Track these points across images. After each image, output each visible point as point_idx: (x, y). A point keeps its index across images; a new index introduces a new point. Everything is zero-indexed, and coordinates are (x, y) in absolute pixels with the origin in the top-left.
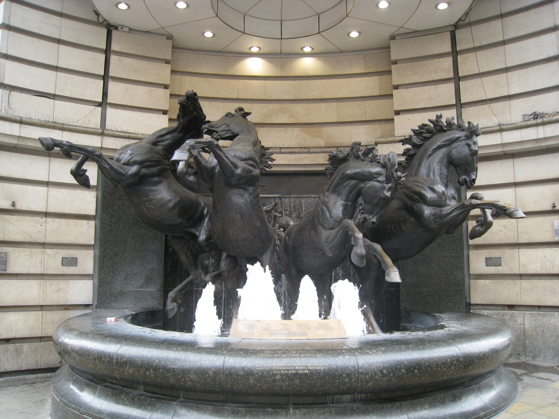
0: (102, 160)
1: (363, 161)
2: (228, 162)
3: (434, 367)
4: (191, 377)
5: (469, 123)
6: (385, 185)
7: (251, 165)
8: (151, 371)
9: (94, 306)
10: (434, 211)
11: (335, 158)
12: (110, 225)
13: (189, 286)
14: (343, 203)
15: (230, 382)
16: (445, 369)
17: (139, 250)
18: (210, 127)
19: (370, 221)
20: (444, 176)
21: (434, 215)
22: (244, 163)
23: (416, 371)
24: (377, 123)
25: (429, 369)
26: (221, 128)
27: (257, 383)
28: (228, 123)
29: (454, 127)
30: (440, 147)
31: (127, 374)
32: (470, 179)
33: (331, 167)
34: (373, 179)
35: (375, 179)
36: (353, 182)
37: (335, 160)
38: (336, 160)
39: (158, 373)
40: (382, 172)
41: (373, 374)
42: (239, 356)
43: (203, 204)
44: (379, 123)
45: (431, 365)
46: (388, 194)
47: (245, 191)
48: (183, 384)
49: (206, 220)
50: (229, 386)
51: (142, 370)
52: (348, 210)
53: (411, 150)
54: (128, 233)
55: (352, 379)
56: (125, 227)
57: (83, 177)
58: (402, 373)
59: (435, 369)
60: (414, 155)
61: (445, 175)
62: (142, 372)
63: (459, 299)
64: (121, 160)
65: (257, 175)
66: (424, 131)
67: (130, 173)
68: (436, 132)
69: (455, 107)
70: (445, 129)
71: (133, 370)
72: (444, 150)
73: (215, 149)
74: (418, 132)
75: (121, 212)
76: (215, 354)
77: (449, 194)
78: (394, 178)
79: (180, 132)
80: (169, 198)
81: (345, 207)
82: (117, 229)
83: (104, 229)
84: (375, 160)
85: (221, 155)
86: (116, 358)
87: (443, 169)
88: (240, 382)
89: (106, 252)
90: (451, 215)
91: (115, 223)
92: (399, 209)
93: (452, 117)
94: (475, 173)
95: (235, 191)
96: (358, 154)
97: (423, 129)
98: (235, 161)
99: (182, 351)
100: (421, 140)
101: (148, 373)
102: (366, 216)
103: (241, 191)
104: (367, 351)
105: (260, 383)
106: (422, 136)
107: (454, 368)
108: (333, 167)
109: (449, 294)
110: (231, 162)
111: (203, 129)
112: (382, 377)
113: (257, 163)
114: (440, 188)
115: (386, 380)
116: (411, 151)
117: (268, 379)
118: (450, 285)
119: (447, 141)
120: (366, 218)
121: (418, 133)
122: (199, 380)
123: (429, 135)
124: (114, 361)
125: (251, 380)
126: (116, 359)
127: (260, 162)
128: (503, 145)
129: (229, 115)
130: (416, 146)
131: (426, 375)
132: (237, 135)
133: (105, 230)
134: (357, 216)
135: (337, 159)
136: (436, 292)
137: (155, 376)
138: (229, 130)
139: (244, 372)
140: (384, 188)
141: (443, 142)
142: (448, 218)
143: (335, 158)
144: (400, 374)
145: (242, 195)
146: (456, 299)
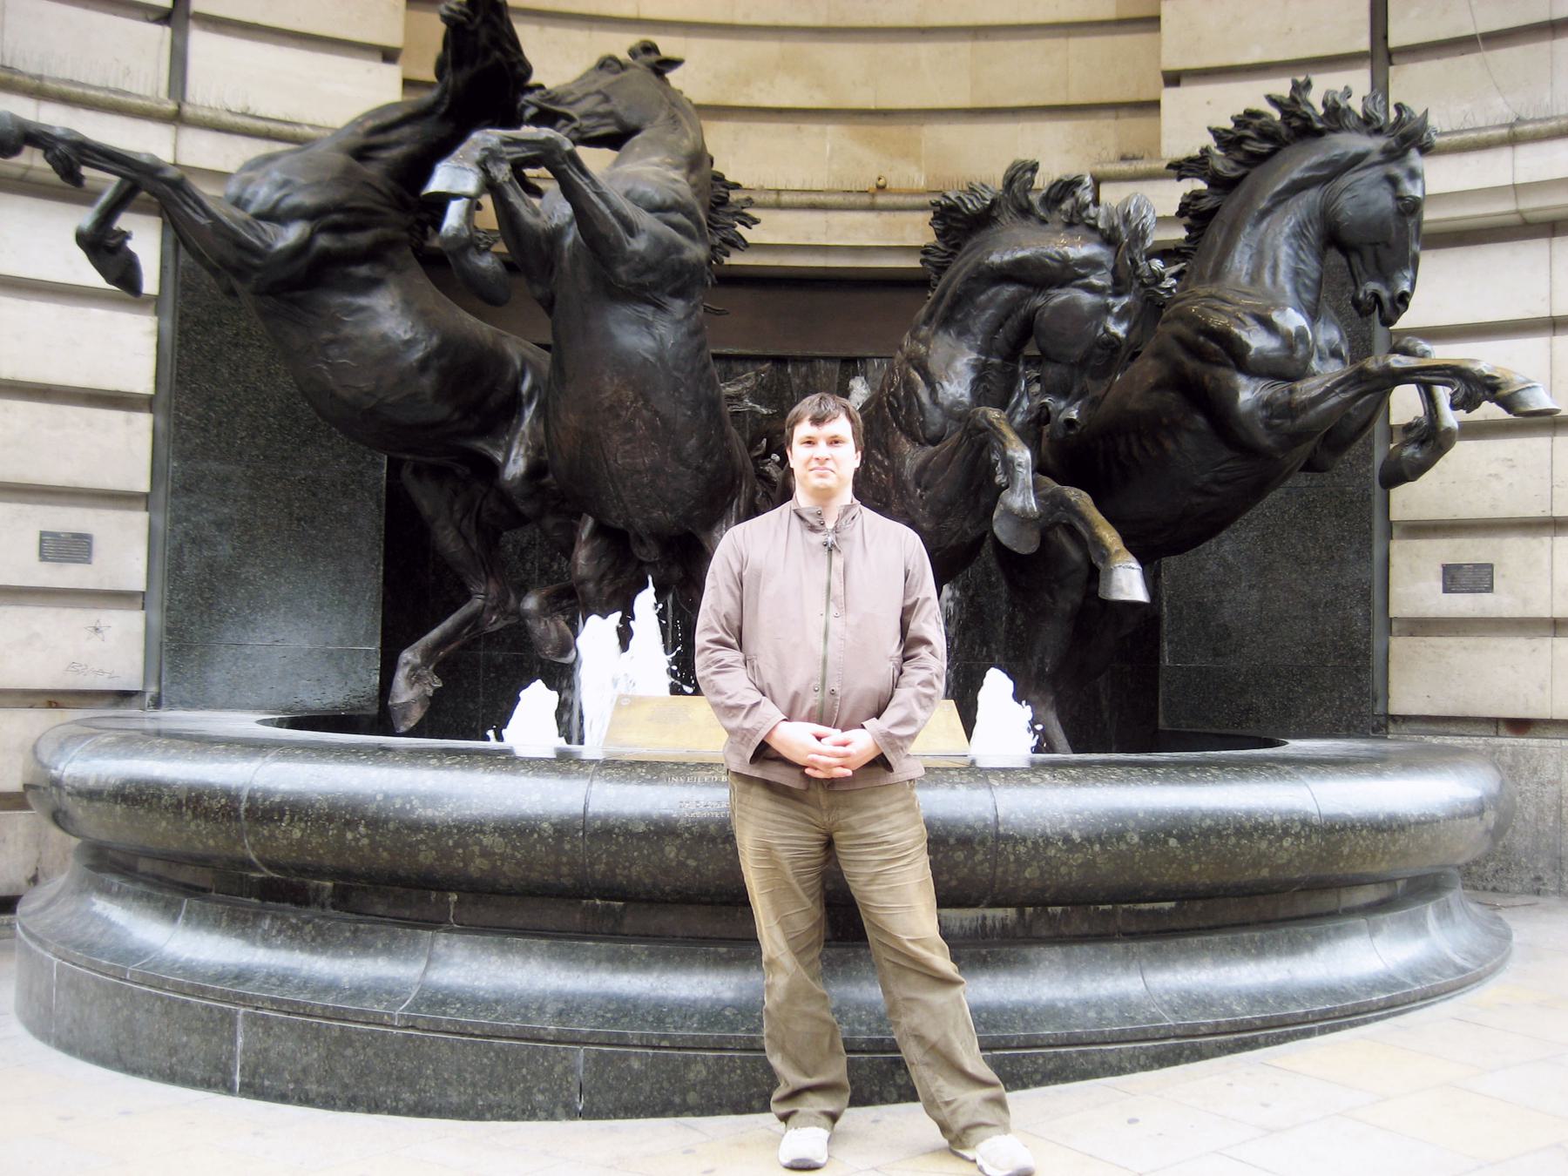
0: (188, 200)
1: (1043, 221)
2: (607, 212)
3: (1228, 835)
4: (486, 841)
5: (1400, 108)
6: (1111, 300)
7: (676, 227)
8: (362, 829)
9: (148, 697)
10: (1267, 394)
11: (954, 215)
12: (205, 430)
13: (466, 631)
14: (976, 360)
15: (604, 856)
16: (1264, 845)
17: (301, 514)
18: (546, 101)
19: (1061, 416)
20: (1307, 281)
21: (1267, 404)
22: (659, 218)
23: (1173, 842)
24: (1103, 114)
25: (1213, 840)
26: (587, 105)
27: (687, 858)
28: (604, 90)
29: (1350, 121)
30: (1297, 188)
31: (285, 842)
33: (941, 246)
34: (1072, 280)
35: (1079, 282)
36: (1008, 291)
37: (954, 219)
38: (959, 221)
39: (382, 835)
40: (1104, 259)
41: (1040, 840)
42: (632, 779)
43: (518, 363)
44: (1112, 113)
45: (1220, 828)
46: (1119, 330)
47: (659, 312)
48: (461, 865)
49: (529, 413)
50: (602, 867)
51: (332, 826)
52: (990, 381)
53: (1204, 197)
54: (265, 457)
55: (974, 855)
56: (253, 437)
58: (1128, 844)
59: (1233, 840)
60: (1213, 212)
61: (1309, 278)
62: (330, 833)
63: (1352, 700)
64: (248, 202)
65: (699, 261)
66: (1249, 133)
67: (280, 245)
68: (1288, 136)
69: (1368, 64)
70: (1319, 126)
71: (303, 830)
72: (1313, 195)
74: (1231, 136)
75: (240, 389)
76: (560, 773)
77: (1321, 343)
78: (1139, 277)
79: (445, 117)
80: (407, 336)
81: (981, 374)
82: (228, 444)
84: (1082, 220)
85: (585, 187)
86: (249, 798)
87: (1303, 256)
88: (636, 854)
90: (1323, 406)
91: (220, 423)
92: (1158, 387)
93: (1346, 88)
94: (1409, 274)
95: (626, 311)
97: (1246, 126)
98: (628, 209)
99: (457, 766)
100: (1238, 162)
101: (349, 836)
102: (1046, 400)
103: (648, 312)
104: (1025, 776)
105: (696, 859)
106: (1241, 149)
107: (1292, 843)
108: (946, 243)
109: (1321, 681)
110: (618, 214)
111: (524, 107)
112: (1066, 851)
113: (698, 223)
114: (1293, 320)
115: (1080, 861)
116: (1204, 200)
117: (721, 846)
118: (1322, 653)
120: (1047, 408)
121: (1230, 142)
122: (509, 850)
123: (1266, 147)
124: (243, 806)
125: (667, 849)
126: (250, 798)
127: (709, 225)
128: (1517, 189)
129: (609, 66)
130: (1223, 185)
131: (1204, 858)
132: (635, 131)
133: (187, 445)
134: (1018, 403)
135: (960, 216)
137: (374, 846)
138: (610, 114)
139: (647, 825)
140: (1107, 309)
141: (1310, 168)
142: (1312, 413)
143: (954, 215)
144: (1123, 847)
145: (648, 325)
146: (1340, 697)
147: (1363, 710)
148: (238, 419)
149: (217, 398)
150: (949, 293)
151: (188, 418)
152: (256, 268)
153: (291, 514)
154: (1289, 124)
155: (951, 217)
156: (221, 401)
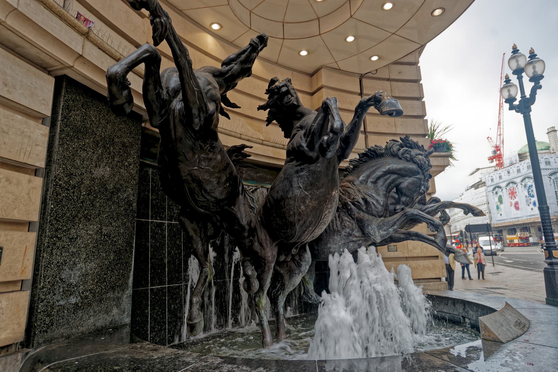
12: (67, 189)
82: (77, 197)
83: (57, 196)
89: (57, 237)
133: (59, 197)
149: (74, 174)
151: (60, 182)
153: (102, 232)
156: (75, 175)
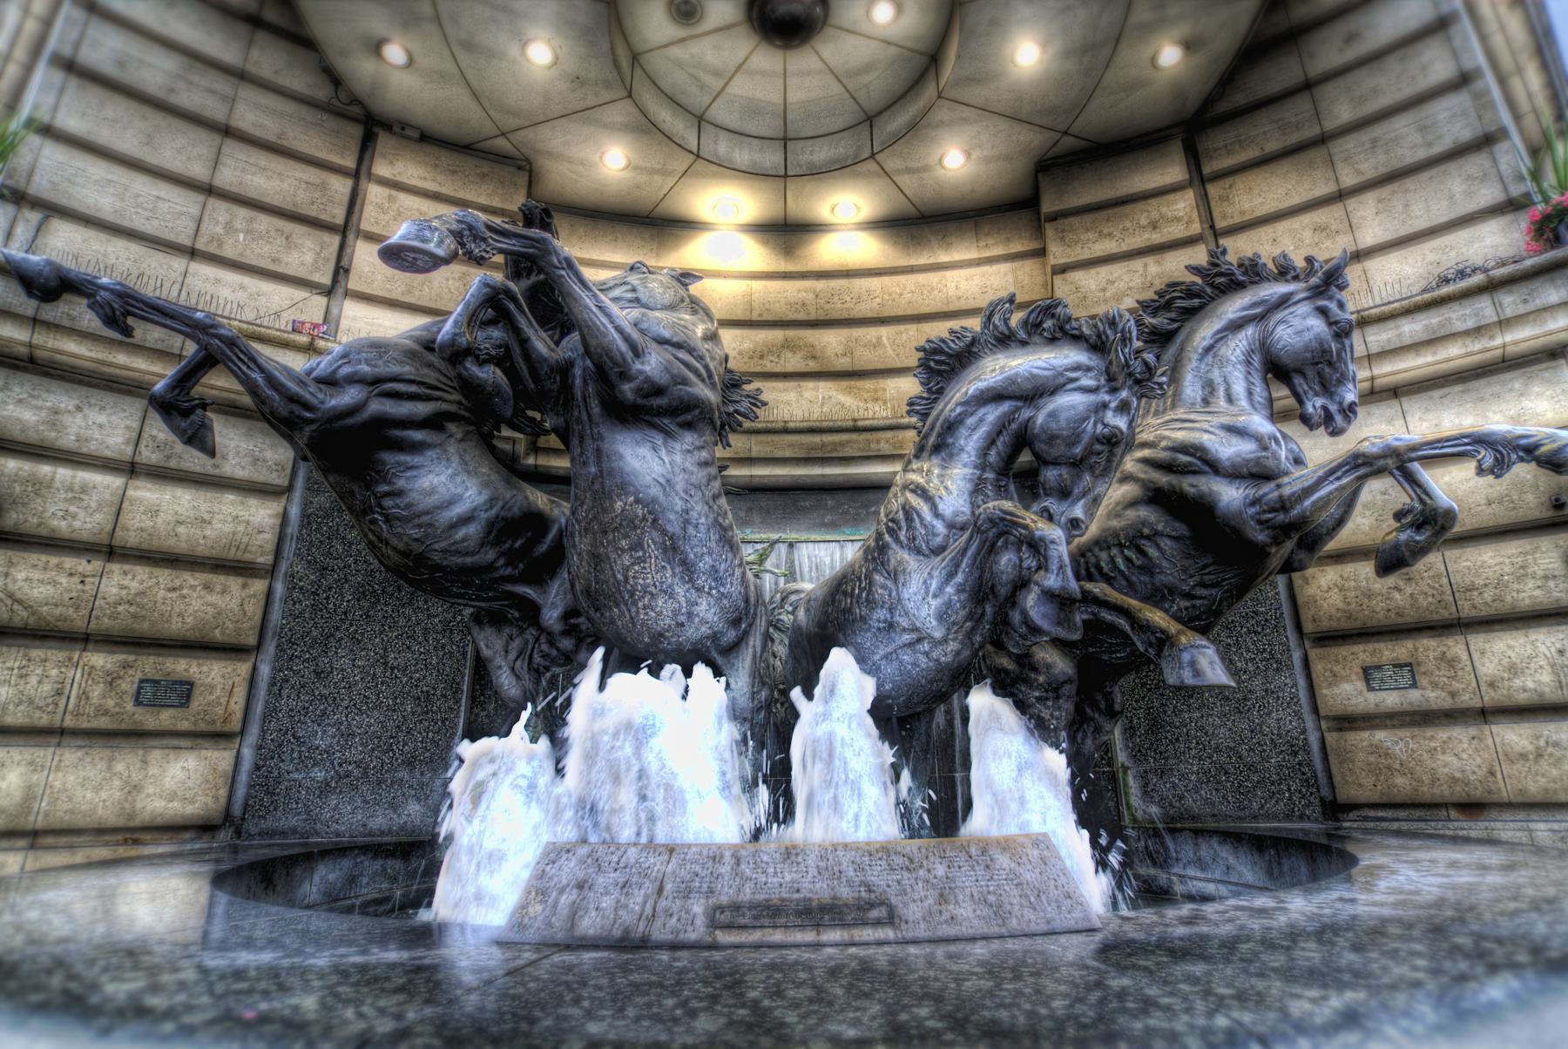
2: (610, 326)
30: (1236, 326)
32: (1341, 404)
34: (1064, 385)
35: (1069, 386)
37: (937, 362)
54: (368, 616)
57: (193, 417)
63: (1300, 792)
72: (1250, 331)
73: (563, 272)
82: (335, 605)
89: (291, 669)
91: (330, 589)
96: (1009, 328)
118: (1264, 751)
119: (1254, 305)
123: (1196, 302)
136: (1226, 773)
146: (1289, 790)
147: (1312, 799)
148: (347, 586)
150: (941, 419)
152: (311, 421)
153: (386, 664)
154: (1212, 285)
155: (934, 360)
